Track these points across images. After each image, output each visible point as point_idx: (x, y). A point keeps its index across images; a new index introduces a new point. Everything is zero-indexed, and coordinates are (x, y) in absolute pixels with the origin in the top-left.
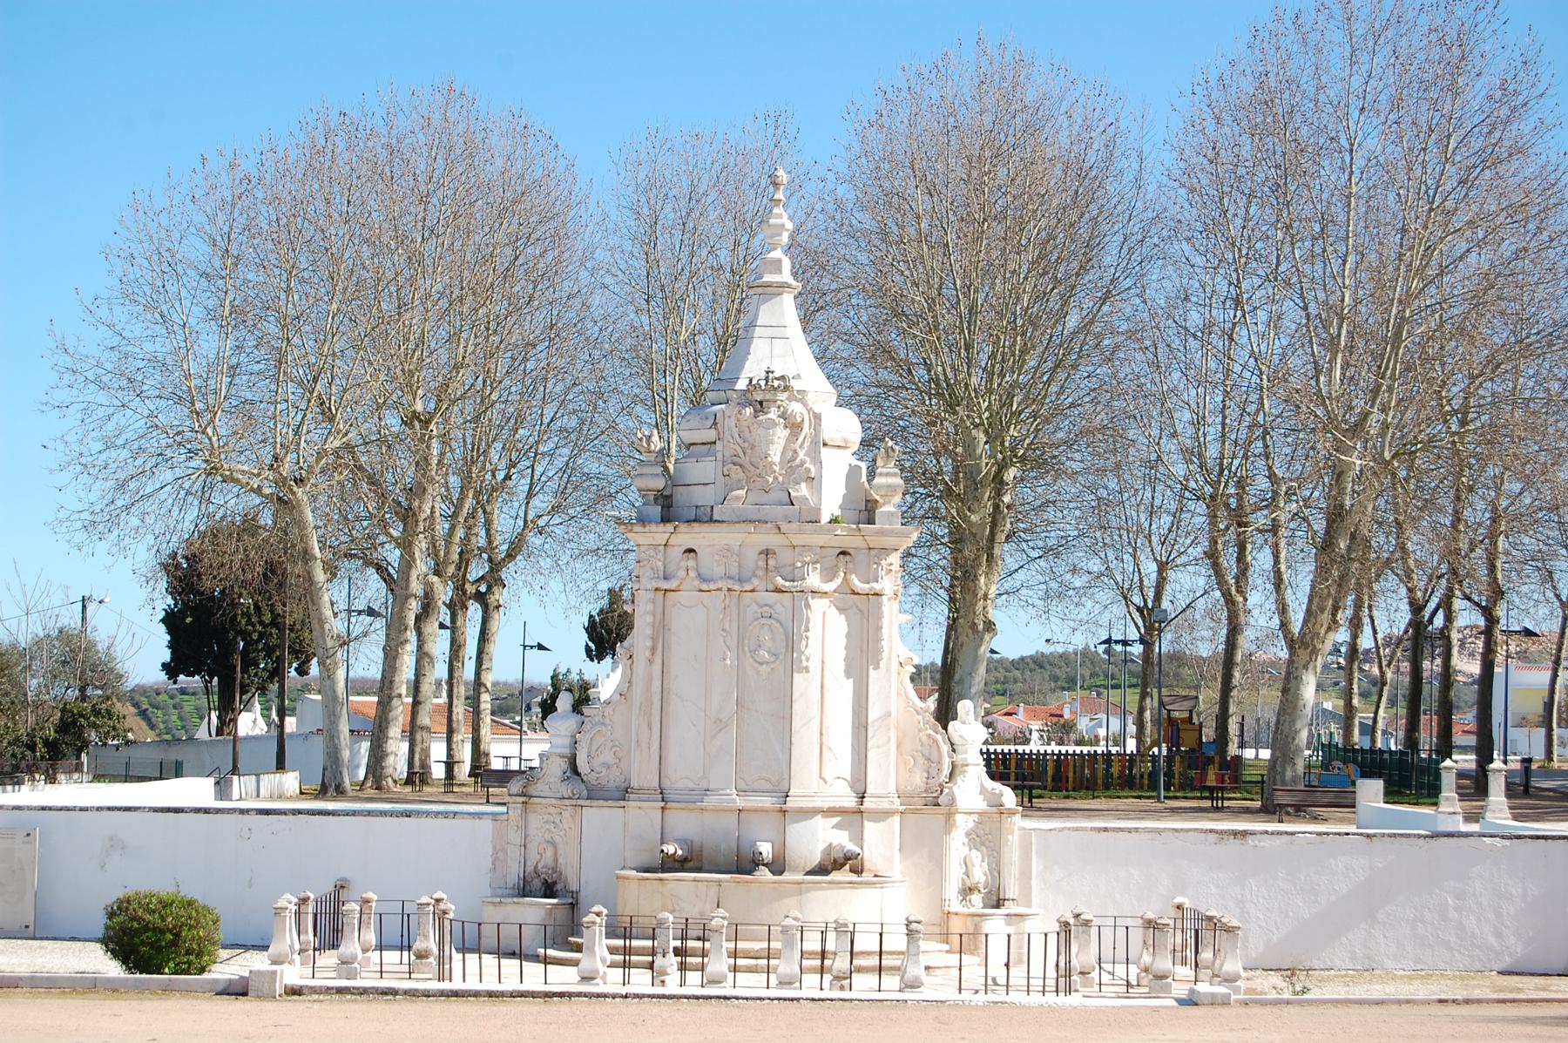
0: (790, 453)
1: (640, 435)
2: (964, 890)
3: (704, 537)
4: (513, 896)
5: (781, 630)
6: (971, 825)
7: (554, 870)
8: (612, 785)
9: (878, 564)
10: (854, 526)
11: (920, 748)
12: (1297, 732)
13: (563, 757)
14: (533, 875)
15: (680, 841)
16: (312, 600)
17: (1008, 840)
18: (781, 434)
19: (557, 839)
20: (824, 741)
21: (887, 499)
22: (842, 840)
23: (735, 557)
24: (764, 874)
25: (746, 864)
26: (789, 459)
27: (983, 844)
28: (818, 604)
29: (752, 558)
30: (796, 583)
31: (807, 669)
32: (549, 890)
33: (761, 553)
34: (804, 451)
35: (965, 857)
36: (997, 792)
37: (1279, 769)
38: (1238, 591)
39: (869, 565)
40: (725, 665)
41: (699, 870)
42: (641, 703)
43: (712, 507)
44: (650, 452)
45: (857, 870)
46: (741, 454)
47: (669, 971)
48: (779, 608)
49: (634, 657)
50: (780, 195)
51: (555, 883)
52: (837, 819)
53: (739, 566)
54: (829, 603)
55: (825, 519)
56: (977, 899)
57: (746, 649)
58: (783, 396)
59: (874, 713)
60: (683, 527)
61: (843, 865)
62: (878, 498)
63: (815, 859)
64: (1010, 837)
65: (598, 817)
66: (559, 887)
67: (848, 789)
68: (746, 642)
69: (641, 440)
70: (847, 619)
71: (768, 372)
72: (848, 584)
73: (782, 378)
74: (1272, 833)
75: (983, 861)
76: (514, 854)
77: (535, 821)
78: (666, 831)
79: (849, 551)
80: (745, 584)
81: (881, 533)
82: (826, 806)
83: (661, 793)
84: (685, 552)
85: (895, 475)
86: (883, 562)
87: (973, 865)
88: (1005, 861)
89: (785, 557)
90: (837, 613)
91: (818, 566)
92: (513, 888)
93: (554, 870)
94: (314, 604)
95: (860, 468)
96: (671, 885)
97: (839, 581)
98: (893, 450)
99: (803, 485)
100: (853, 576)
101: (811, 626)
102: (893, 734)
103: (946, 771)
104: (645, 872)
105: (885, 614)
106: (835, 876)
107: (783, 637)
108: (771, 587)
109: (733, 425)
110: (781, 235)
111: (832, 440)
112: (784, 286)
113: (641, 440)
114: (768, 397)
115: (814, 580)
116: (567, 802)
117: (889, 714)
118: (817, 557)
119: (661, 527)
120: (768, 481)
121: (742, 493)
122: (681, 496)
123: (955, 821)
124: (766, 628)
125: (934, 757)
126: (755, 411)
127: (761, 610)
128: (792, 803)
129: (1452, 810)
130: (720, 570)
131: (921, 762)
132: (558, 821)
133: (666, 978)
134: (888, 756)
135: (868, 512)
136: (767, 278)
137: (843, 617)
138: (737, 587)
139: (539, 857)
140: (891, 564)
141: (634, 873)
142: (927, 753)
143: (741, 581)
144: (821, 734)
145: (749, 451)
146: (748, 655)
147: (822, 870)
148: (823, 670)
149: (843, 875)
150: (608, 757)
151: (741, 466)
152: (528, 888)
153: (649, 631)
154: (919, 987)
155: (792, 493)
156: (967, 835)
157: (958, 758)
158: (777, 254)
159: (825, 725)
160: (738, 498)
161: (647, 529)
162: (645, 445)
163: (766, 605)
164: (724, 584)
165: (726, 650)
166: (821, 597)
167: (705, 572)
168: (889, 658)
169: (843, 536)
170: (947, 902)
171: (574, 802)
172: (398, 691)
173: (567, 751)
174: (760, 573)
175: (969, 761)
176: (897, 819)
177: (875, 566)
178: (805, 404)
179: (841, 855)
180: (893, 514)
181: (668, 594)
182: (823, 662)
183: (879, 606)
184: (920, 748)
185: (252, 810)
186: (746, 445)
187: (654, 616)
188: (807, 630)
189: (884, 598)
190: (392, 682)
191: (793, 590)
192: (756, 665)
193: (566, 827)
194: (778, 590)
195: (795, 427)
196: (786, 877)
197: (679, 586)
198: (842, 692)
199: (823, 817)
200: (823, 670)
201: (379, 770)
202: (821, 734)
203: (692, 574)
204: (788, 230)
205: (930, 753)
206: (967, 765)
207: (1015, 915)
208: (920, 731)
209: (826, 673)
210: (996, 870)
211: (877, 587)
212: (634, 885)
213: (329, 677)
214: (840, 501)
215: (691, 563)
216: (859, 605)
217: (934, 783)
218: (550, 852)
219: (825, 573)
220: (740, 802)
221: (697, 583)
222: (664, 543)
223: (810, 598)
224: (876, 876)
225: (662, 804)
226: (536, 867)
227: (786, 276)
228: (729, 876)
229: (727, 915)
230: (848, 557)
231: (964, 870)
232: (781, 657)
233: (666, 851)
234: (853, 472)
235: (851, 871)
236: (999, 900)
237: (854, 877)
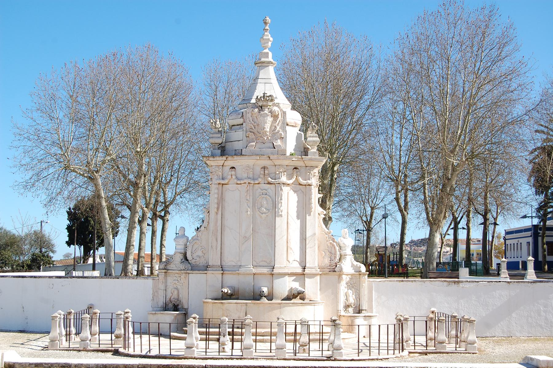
0: (274, 127)
1: (212, 121)
2: (346, 306)
3: (238, 162)
4: (161, 311)
5: (271, 199)
6: (348, 279)
7: (178, 300)
8: (201, 264)
9: (310, 173)
10: (300, 157)
11: (327, 248)
12: (434, 253)
13: (181, 253)
14: (169, 302)
15: (230, 287)
16: (101, 212)
17: (363, 286)
18: (270, 119)
19: (179, 287)
20: (289, 245)
21: (313, 146)
22: (296, 286)
23: (251, 170)
24: (264, 300)
25: (257, 296)
26: (273, 130)
27: (353, 287)
28: (286, 189)
29: (258, 170)
30: (276, 180)
31: (281, 216)
32: (176, 308)
33: (262, 168)
34: (279, 127)
35: (346, 293)
36: (358, 266)
37: (428, 266)
38: (405, 210)
39: (306, 173)
40: (248, 214)
41: (238, 299)
42: (213, 230)
43: (242, 150)
44: (216, 128)
45: (303, 299)
46: (253, 128)
47: (226, 343)
48: (269, 190)
49: (210, 212)
50: (267, 28)
51: (178, 305)
52: (294, 277)
53: (253, 174)
54: (290, 189)
55: (288, 154)
56: (351, 310)
57: (256, 207)
58: (270, 104)
59: (309, 234)
60: (230, 158)
61: (297, 296)
62: (309, 147)
63: (285, 294)
64: (364, 284)
65: (196, 278)
66: (180, 307)
67: (299, 265)
68: (256, 204)
69: (212, 123)
71: (264, 94)
72: (298, 181)
73: (270, 96)
74: (470, 282)
75: (353, 294)
76: (161, 293)
77: (170, 280)
78: (224, 283)
79: (298, 167)
80: (256, 181)
81: (311, 160)
82: (290, 272)
83: (221, 267)
84: (231, 168)
85: (316, 137)
86: (312, 172)
87: (349, 296)
88: (362, 294)
89: (272, 169)
90: (293, 193)
91: (285, 173)
92: (161, 308)
93: (178, 300)
94: (102, 213)
95: (302, 134)
96: (226, 305)
97: (294, 179)
98: (315, 127)
99: (279, 141)
100: (300, 178)
101: (283, 198)
102: (316, 242)
103: (338, 258)
104: (215, 300)
105: (313, 193)
106: (293, 301)
107: (271, 202)
108: (266, 182)
109: (250, 116)
110: (268, 43)
111: (290, 123)
112: (270, 63)
113: (212, 123)
114: (265, 103)
115: (284, 179)
116: (183, 272)
117: (315, 234)
118: (285, 170)
119: (221, 158)
120: (264, 139)
121: (254, 144)
122: (229, 146)
123: (342, 278)
124: (264, 199)
125: (333, 252)
126: (259, 110)
127: (262, 191)
128: (275, 271)
129: (505, 276)
130: (245, 175)
131: (328, 254)
132: (179, 280)
133: (225, 347)
134: (314, 251)
135: (306, 152)
136: (263, 60)
137: (296, 194)
138: (252, 182)
139: (171, 294)
141: (211, 300)
142: (330, 250)
143: (254, 179)
144: (287, 242)
146: (257, 210)
147: (288, 298)
148: (288, 216)
149: (297, 300)
150: (199, 253)
151: (253, 133)
152: (167, 307)
153: (216, 201)
154: (340, 350)
155: (274, 144)
156: (347, 283)
157: (343, 253)
158: (266, 51)
159: (289, 238)
160: (252, 146)
161: (215, 159)
162: (214, 125)
163: (264, 189)
164: (247, 181)
165: (248, 208)
166: (286, 186)
167: (239, 176)
168: (315, 211)
169: (296, 161)
170: (339, 311)
171: (185, 272)
172: (132, 244)
173: (183, 251)
174: (262, 176)
175: (347, 253)
176: (318, 277)
177: (309, 174)
178: (279, 107)
179: (296, 292)
180: (315, 153)
181: (224, 185)
182: (288, 213)
184: (327, 248)
185: (54, 276)
186: (255, 124)
187: (218, 194)
188: (281, 199)
190: (130, 241)
191: (275, 183)
192: (260, 214)
193: (182, 282)
194: (269, 183)
195: (275, 117)
196: (274, 301)
197: (228, 182)
198: (296, 225)
199: (288, 276)
200: (288, 216)
201: (126, 270)
202: (287, 242)
203: (234, 177)
204: (271, 41)
205: (331, 250)
206: (346, 255)
207: (367, 316)
208: (327, 241)
209: (289, 217)
210: (358, 298)
211: (309, 182)
212: (210, 306)
213: (107, 238)
214: (294, 147)
215: (233, 173)
217: (333, 263)
218: (176, 292)
219: (288, 176)
220: (254, 271)
221: (236, 180)
222: (222, 165)
223: (282, 186)
224: (310, 301)
225: (222, 272)
226: (170, 299)
227: (270, 59)
228: (250, 301)
229: (252, 318)
230: (297, 170)
231: (345, 298)
232: (271, 211)
233: (224, 291)
234: (298, 137)
235: (300, 299)
236: (360, 310)
237: (301, 301)
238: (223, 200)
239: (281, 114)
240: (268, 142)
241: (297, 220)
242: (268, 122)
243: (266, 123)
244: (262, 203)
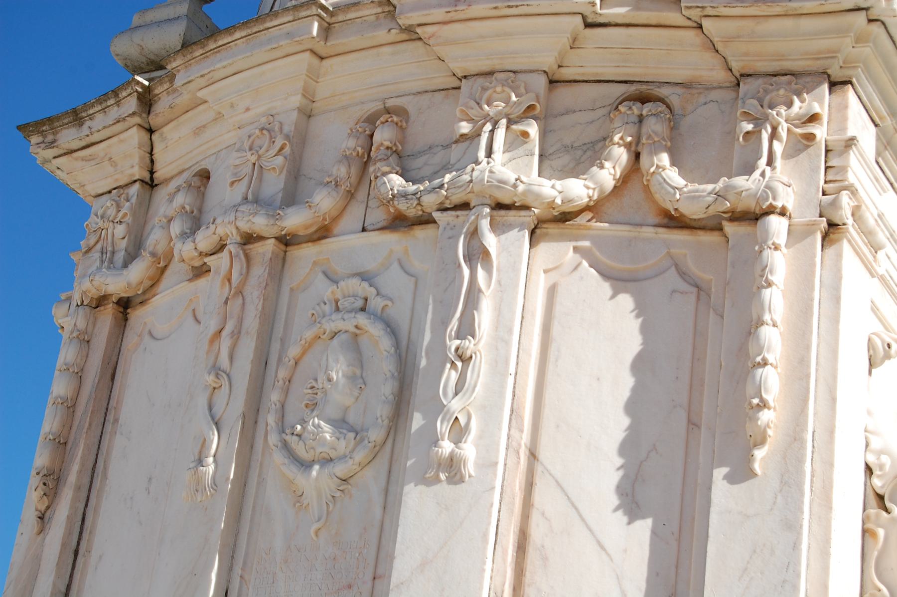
5: (386, 343)
40: (199, 480)
68: (274, 396)
70: (641, 309)
79: (664, 92)
90: (606, 288)
100: (664, 158)
108: (378, 216)
137: (626, 301)
140: (814, 118)
182: (533, 455)
183: (762, 243)
188: (467, 329)
189: (777, 225)
209: (543, 496)
216: (692, 267)
222: (138, 172)
223: (485, 224)
238: (110, 417)
241: (621, 517)
244: (322, 378)
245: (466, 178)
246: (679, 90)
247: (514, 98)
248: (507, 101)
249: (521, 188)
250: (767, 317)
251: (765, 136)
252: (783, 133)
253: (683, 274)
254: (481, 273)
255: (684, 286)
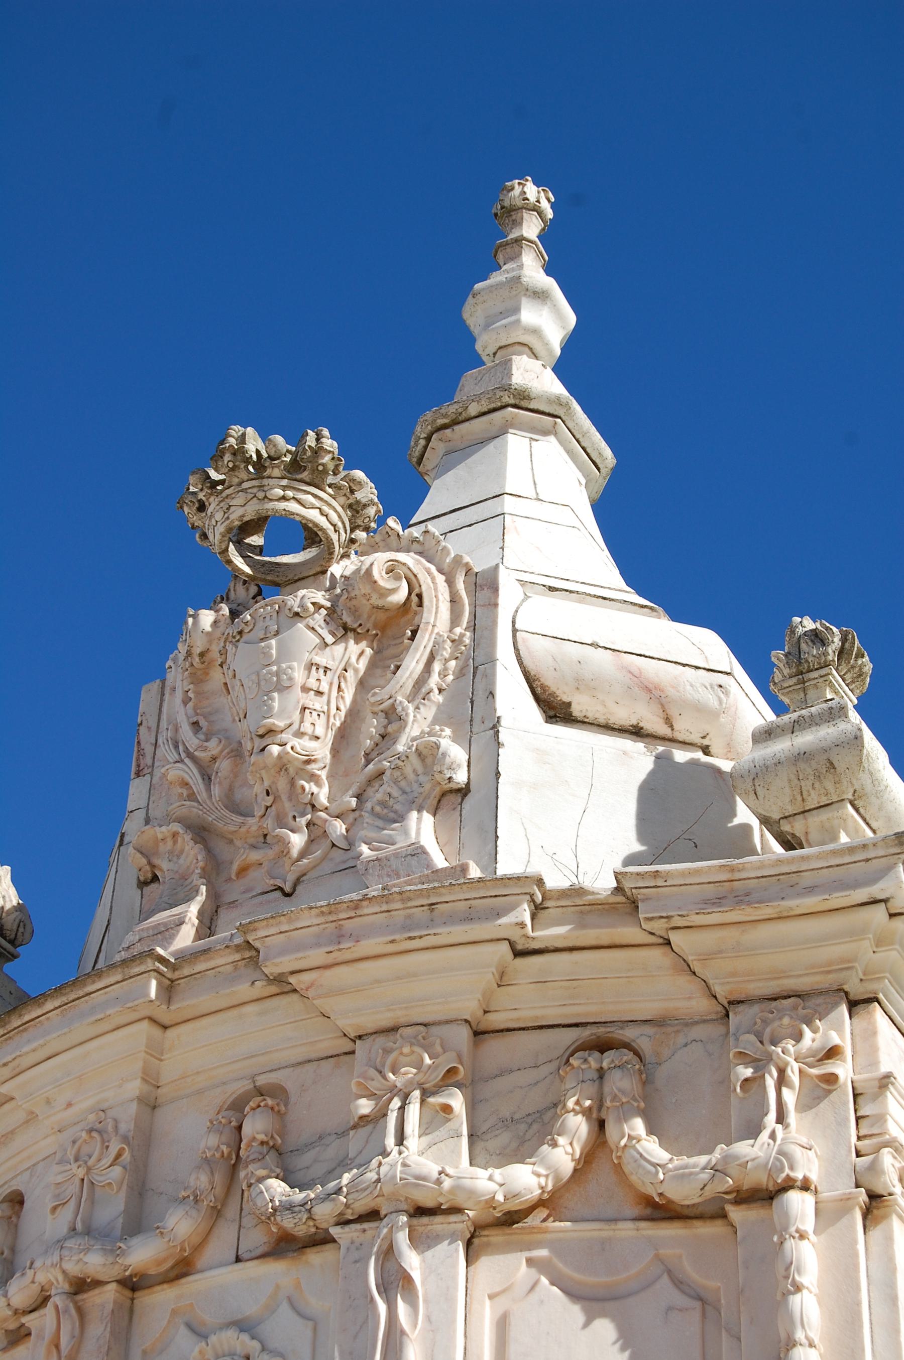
0: (372, 726)
34: (428, 712)
79: (629, 1034)
90: (576, 1312)
100: (638, 1126)
137: (605, 1329)
140: (832, 1053)
145: (224, 766)
186: (214, 747)
223: (402, 1238)
239: (454, 600)
240: (327, 867)
242: (299, 675)
243: (282, 688)
245: (372, 1176)
246: (649, 1030)
247: (428, 1061)
248: (419, 1065)
249: (447, 1183)
250: (800, 1335)
251: (770, 1083)
252: (793, 1075)
253: (679, 1283)
254: (402, 1308)
255: (680, 1300)
